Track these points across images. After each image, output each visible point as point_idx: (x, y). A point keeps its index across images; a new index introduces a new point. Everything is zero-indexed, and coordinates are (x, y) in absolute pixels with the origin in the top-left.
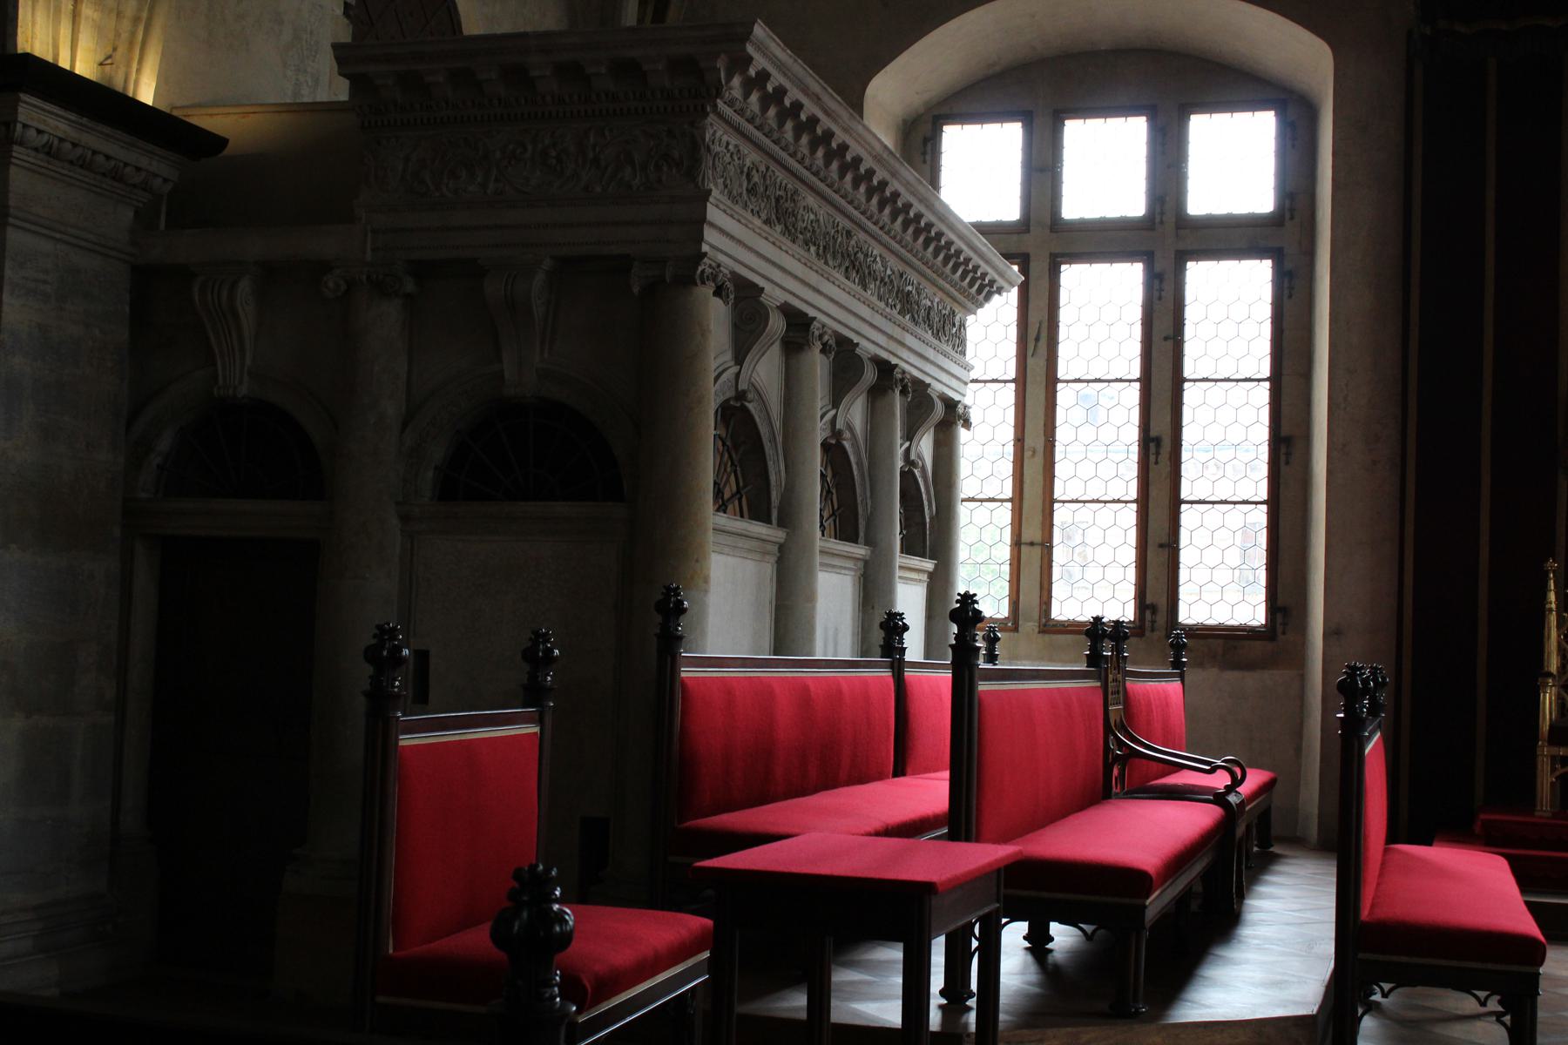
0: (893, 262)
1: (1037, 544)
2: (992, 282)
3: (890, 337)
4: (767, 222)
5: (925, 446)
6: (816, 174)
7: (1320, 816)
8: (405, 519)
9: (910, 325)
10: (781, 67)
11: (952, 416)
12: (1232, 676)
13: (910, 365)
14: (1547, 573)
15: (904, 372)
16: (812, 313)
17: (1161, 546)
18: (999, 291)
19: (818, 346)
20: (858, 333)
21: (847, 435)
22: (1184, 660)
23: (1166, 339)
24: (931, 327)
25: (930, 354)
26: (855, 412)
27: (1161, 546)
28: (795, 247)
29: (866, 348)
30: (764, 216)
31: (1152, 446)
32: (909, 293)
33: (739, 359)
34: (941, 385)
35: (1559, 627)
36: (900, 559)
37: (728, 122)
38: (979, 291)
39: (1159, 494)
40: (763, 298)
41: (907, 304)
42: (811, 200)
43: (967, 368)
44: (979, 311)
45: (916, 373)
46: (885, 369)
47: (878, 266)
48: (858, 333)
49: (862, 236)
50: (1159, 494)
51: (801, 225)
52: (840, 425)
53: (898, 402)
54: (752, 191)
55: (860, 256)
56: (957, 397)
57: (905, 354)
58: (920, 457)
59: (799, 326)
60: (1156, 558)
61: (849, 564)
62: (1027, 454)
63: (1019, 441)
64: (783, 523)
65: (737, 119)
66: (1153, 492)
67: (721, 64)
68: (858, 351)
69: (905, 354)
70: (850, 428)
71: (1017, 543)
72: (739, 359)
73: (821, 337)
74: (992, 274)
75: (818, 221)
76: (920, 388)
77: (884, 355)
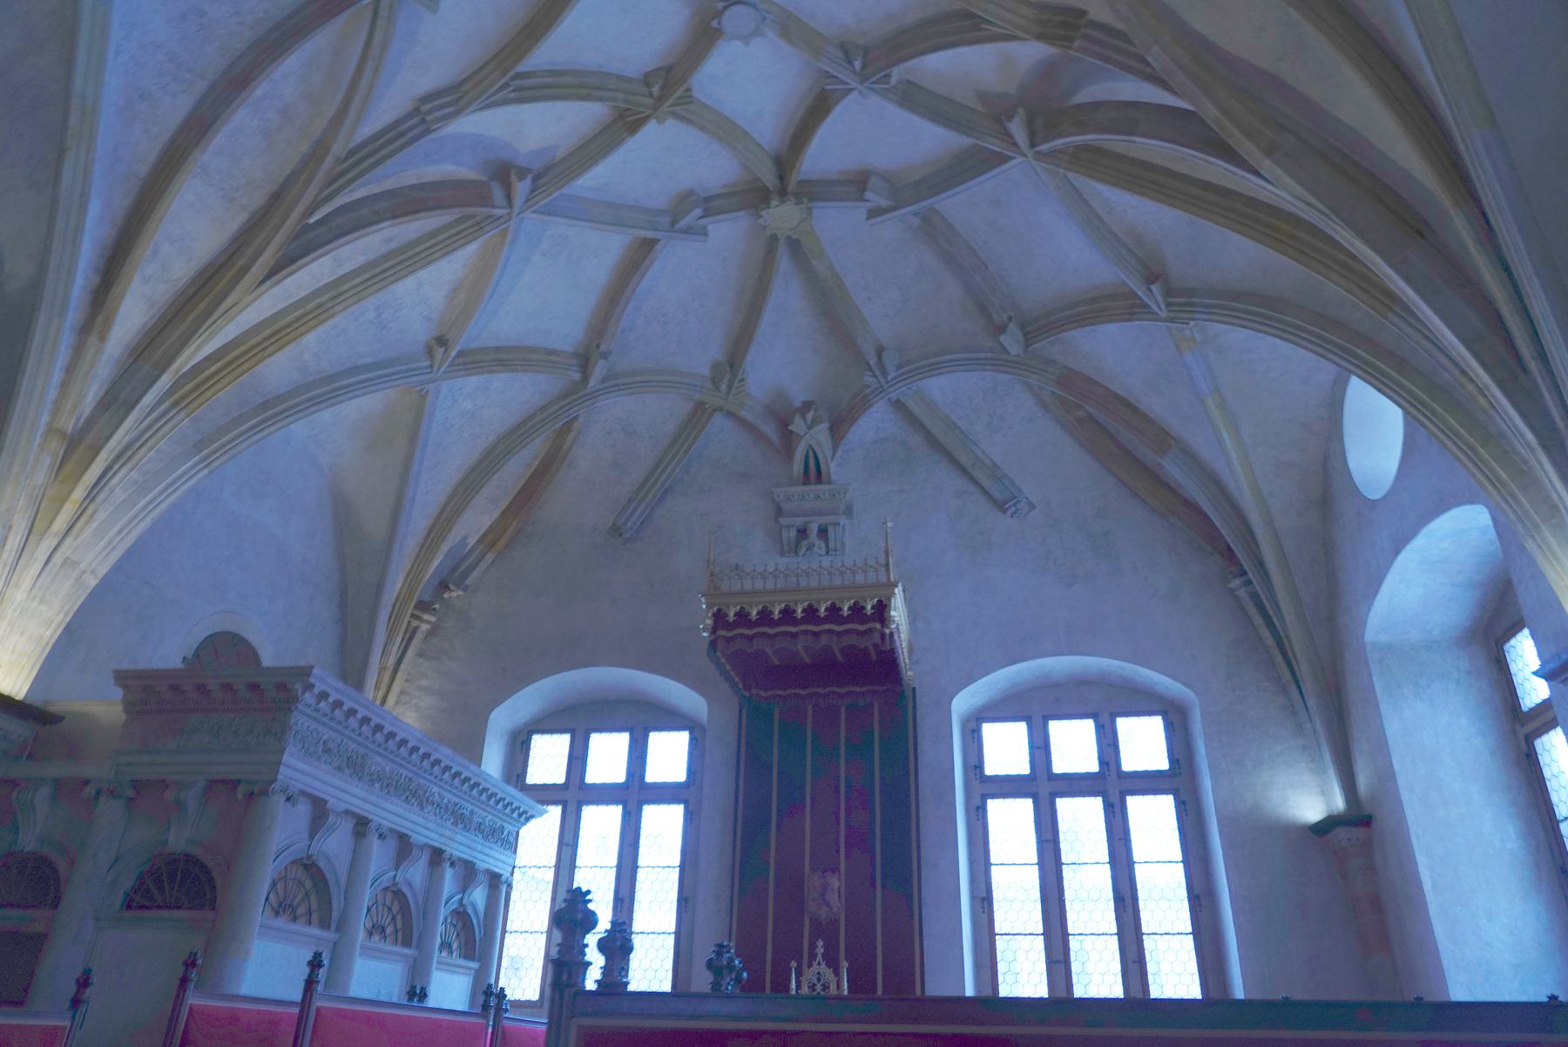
4: (339, 768)
5: (478, 896)
8: (97, 919)
10: (337, 690)
14: (791, 969)
30: (336, 765)
31: (620, 902)
33: (312, 836)
37: (309, 716)
40: (328, 806)
42: (379, 759)
49: (422, 781)
54: (327, 751)
59: (361, 825)
64: (338, 930)
65: (314, 714)
67: (298, 687)
70: (409, 884)
72: (312, 836)
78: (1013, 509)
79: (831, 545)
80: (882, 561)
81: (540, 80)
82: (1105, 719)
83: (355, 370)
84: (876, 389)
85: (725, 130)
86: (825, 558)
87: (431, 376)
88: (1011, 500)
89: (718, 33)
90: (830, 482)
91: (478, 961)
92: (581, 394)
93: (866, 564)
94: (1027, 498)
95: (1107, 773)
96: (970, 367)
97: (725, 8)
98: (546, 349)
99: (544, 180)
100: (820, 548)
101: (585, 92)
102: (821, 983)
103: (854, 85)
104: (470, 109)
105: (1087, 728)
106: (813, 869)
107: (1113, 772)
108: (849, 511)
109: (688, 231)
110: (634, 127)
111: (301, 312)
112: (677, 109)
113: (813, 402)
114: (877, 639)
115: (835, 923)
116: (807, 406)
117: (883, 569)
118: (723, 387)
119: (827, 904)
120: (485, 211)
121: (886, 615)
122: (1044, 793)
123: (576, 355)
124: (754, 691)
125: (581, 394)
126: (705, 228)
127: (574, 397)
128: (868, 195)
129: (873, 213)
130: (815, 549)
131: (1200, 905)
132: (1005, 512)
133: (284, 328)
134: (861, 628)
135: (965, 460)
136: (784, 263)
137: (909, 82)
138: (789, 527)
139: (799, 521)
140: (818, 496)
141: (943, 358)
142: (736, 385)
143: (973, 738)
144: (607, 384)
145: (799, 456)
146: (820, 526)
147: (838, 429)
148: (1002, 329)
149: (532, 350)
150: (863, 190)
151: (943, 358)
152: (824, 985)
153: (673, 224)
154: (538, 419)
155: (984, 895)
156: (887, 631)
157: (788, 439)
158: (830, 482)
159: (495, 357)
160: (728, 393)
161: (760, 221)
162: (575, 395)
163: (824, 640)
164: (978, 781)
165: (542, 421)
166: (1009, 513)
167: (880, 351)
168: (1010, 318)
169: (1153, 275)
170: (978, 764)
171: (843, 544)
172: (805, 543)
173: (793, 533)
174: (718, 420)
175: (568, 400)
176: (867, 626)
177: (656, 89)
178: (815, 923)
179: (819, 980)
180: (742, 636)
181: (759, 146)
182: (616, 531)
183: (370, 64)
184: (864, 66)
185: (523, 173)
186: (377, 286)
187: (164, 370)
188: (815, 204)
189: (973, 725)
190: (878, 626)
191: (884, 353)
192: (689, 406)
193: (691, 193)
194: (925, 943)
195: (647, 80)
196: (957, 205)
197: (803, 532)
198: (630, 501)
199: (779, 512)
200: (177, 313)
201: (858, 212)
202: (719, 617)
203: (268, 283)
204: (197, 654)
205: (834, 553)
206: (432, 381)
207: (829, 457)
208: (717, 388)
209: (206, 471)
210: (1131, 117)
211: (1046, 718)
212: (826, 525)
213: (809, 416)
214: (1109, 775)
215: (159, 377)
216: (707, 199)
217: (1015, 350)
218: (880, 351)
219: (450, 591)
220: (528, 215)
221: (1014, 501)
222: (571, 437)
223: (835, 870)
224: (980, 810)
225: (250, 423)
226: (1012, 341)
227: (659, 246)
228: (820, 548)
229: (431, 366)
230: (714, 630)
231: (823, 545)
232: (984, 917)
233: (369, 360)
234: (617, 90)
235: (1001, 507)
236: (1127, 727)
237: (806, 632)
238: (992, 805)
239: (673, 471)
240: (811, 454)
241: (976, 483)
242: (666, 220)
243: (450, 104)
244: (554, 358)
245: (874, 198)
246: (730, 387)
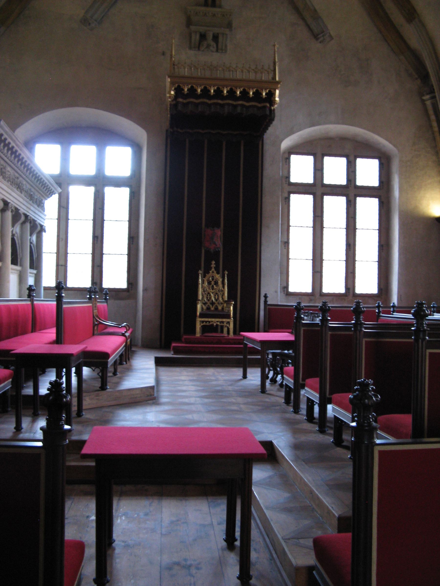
0: (28, 186)
1: (63, 265)
2: (53, 191)
3: (27, 207)
5: (34, 238)
6: (11, 162)
7: (142, 339)
9: (32, 204)
11: (42, 229)
12: (117, 302)
13: (32, 215)
15: (31, 217)
16: (9, 201)
17: (98, 266)
18: (54, 194)
19: (10, 210)
20: (19, 206)
21: (16, 235)
22: (108, 298)
23: (100, 209)
24: (37, 204)
25: (37, 212)
26: (17, 229)
27: (98, 266)
28: (5, 182)
29: (22, 211)
31: (96, 238)
32: (32, 194)
34: (39, 221)
35: (202, 287)
36: (30, 271)
38: (49, 194)
39: (97, 251)
41: (31, 197)
42: (9, 169)
43: (45, 215)
44: (49, 199)
45: (33, 217)
46: (26, 216)
47: (24, 187)
48: (19, 206)
49: (21, 179)
50: (97, 251)
51: (7, 176)
52: (14, 233)
53: (28, 226)
55: (20, 184)
56: (42, 224)
57: (31, 212)
58: (33, 241)
60: (97, 270)
61: (16, 272)
62: (61, 240)
63: (58, 236)
66: (96, 251)
68: (20, 211)
69: (31, 212)
70: (16, 233)
71: (58, 265)
73: (11, 207)
74: (53, 189)
75: (11, 174)
76: (34, 221)
77: (26, 212)
78: (321, 39)
80: (272, 68)
82: (352, 158)
86: (215, 54)
88: (322, 33)
90: (220, 7)
91: (36, 269)
93: (262, 68)
94: (330, 33)
95: (349, 185)
100: (214, 47)
102: (214, 280)
105: (342, 162)
106: (207, 226)
107: (353, 185)
108: (229, 26)
114: (268, 112)
115: (217, 253)
117: (272, 73)
119: (215, 244)
121: (273, 99)
122: (319, 194)
124: (175, 129)
130: (211, 48)
131: (382, 249)
134: (259, 105)
138: (196, 32)
139: (202, 29)
143: (286, 162)
152: (215, 282)
155: (286, 240)
156: (272, 108)
158: (220, 7)
163: (239, 109)
164: (287, 185)
166: (319, 40)
170: (287, 176)
171: (226, 46)
172: (205, 44)
173: (198, 37)
176: (262, 105)
178: (207, 252)
179: (213, 279)
180: (192, 102)
189: (286, 155)
190: (268, 105)
194: (262, 263)
197: (203, 37)
199: (189, 23)
202: (179, 90)
205: (221, 51)
211: (324, 155)
212: (218, 34)
214: (351, 187)
221: (323, 34)
223: (218, 226)
224: (287, 199)
231: (215, 46)
232: (285, 251)
235: (316, 37)
236: (361, 163)
237: (228, 104)
238: (293, 197)
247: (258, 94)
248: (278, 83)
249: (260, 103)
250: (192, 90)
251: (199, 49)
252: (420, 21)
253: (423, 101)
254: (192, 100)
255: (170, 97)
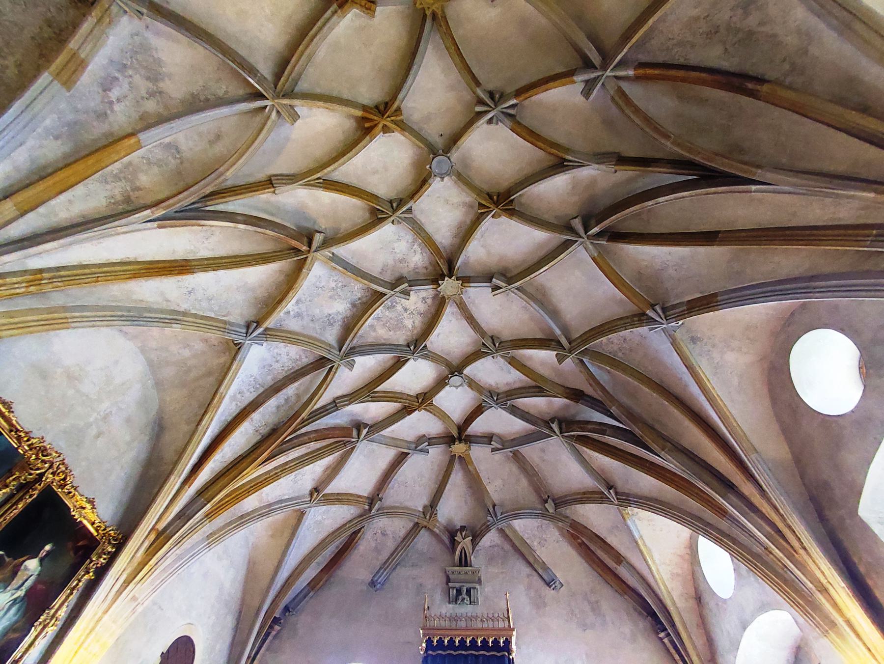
78: (554, 586)
79: (472, 600)
80: (506, 616)
81: (380, 395)
83: (281, 501)
84: (492, 523)
85: (441, 415)
87: (309, 505)
89: (447, 384)
90: (471, 566)
92: (367, 516)
96: (533, 517)
97: (451, 377)
98: (357, 495)
99: (373, 428)
101: (395, 399)
103: (493, 405)
104: (356, 402)
108: (479, 582)
109: (421, 451)
110: (410, 413)
111: (268, 476)
112: (427, 407)
113: (465, 527)
116: (463, 528)
118: (428, 517)
120: (349, 439)
123: (368, 498)
125: (367, 516)
126: (428, 449)
127: (364, 517)
128: (492, 443)
129: (493, 450)
130: (465, 601)
132: (550, 587)
133: (260, 482)
135: (531, 560)
136: (457, 466)
137: (513, 405)
139: (458, 585)
140: (466, 573)
141: (519, 512)
142: (433, 516)
144: (379, 512)
145: (458, 552)
146: (467, 589)
147: (475, 540)
148: (546, 501)
149: (351, 495)
150: (491, 441)
151: (519, 512)
153: (416, 447)
154: (347, 526)
156: (511, 657)
157: (453, 543)
159: (336, 497)
160: (429, 520)
161: (450, 449)
162: (365, 516)
165: (349, 527)
166: (552, 588)
167: (494, 506)
168: (548, 497)
169: (610, 487)
171: (478, 599)
172: (460, 597)
173: (455, 591)
174: (423, 531)
175: (362, 518)
177: (420, 401)
181: (453, 421)
182: (373, 584)
183: (324, 386)
184: (497, 400)
185: (366, 425)
186: (301, 467)
187: (209, 502)
188: (472, 444)
190: (507, 654)
191: (496, 507)
192: (411, 525)
193: (424, 436)
195: (417, 396)
196: (527, 450)
197: (459, 592)
198: (381, 568)
199: (448, 580)
200: (223, 475)
201: (487, 449)
202: (429, 642)
203: (262, 466)
204: (168, 651)
206: (309, 507)
207: (471, 552)
208: (425, 517)
209: (208, 549)
210: (602, 428)
212: (470, 588)
213: (464, 534)
215: (206, 505)
216: (429, 439)
217: (551, 510)
218: (494, 506)
219: (290, 612)
220: (365, 441)
222: (359, 535)
225: (234, 525)
226: (550, 506)
227: (409, 456)
228: (467, 600)
229: (310, 501)
230: (427, 650)
231: (468, 599)
233: (286, 497)
234: (406, 399)
235: (548, 584)
239: (402, 554)
240: (463, 551)
241: (536, 571)
242: (414, 446)
243: (347, 401)
244: (359, 499)
245: (495, 444)
246: (430, 517)
247: (496, 642)
248: (513, 630)
249: (499, 652)
250: (440, 641)
251: (456, 603)
252: (628, 563)
253: (661, 639)
254: (440, 652)
255: (421, 649)
